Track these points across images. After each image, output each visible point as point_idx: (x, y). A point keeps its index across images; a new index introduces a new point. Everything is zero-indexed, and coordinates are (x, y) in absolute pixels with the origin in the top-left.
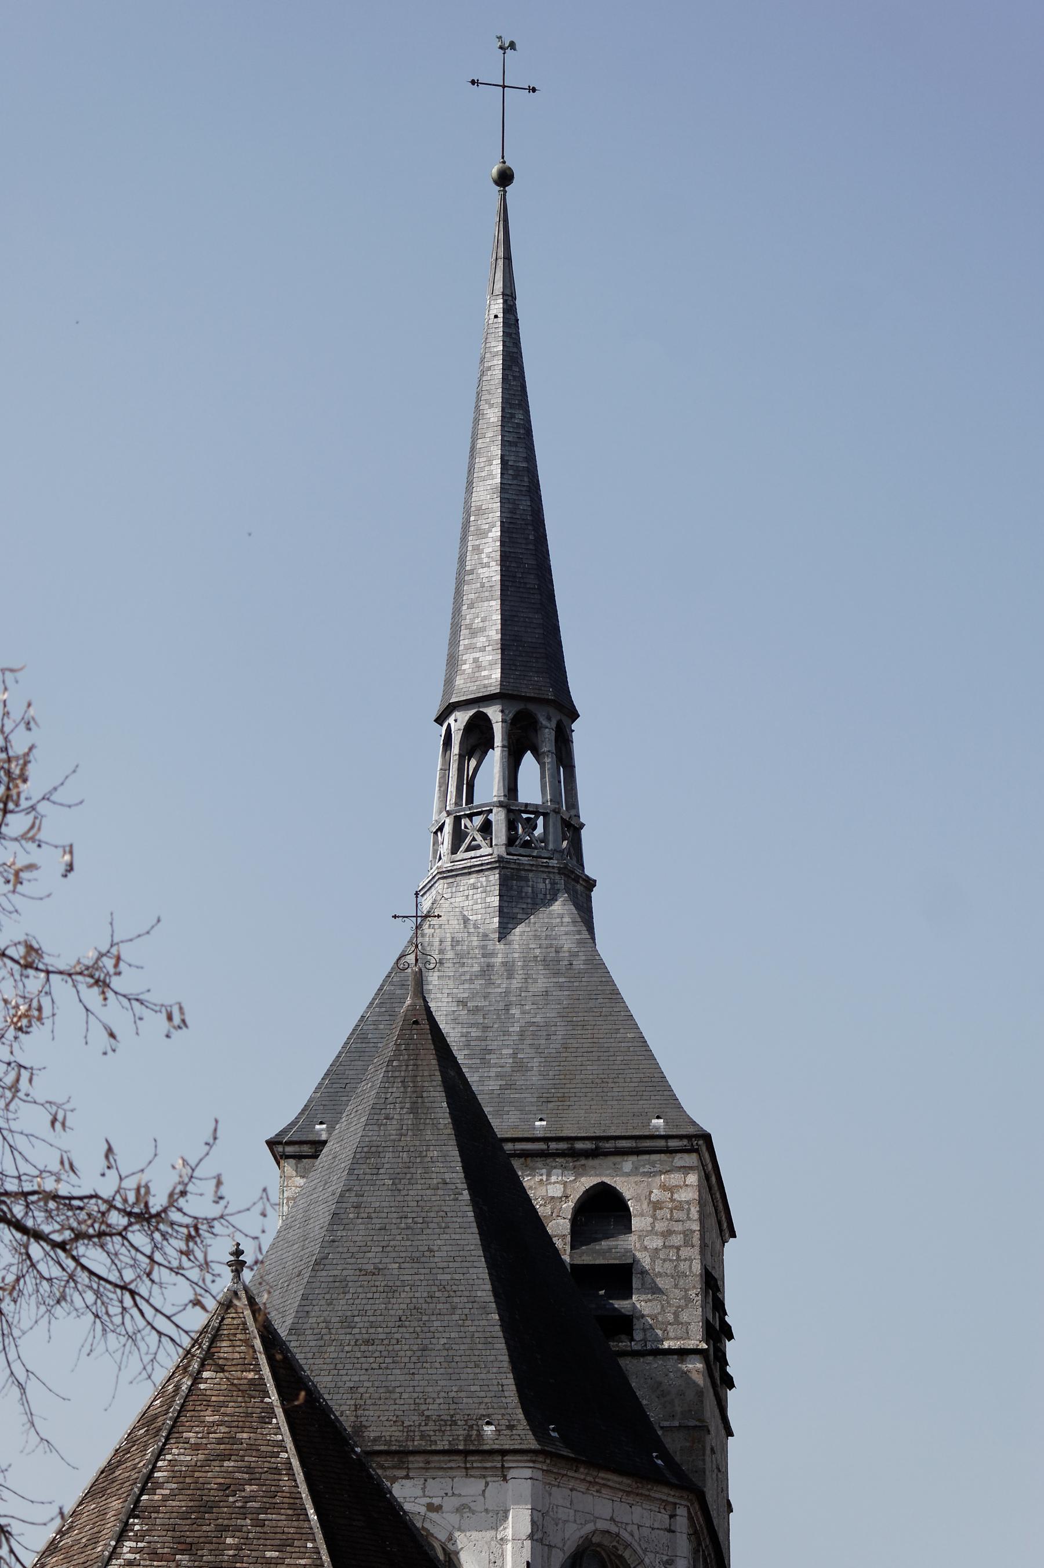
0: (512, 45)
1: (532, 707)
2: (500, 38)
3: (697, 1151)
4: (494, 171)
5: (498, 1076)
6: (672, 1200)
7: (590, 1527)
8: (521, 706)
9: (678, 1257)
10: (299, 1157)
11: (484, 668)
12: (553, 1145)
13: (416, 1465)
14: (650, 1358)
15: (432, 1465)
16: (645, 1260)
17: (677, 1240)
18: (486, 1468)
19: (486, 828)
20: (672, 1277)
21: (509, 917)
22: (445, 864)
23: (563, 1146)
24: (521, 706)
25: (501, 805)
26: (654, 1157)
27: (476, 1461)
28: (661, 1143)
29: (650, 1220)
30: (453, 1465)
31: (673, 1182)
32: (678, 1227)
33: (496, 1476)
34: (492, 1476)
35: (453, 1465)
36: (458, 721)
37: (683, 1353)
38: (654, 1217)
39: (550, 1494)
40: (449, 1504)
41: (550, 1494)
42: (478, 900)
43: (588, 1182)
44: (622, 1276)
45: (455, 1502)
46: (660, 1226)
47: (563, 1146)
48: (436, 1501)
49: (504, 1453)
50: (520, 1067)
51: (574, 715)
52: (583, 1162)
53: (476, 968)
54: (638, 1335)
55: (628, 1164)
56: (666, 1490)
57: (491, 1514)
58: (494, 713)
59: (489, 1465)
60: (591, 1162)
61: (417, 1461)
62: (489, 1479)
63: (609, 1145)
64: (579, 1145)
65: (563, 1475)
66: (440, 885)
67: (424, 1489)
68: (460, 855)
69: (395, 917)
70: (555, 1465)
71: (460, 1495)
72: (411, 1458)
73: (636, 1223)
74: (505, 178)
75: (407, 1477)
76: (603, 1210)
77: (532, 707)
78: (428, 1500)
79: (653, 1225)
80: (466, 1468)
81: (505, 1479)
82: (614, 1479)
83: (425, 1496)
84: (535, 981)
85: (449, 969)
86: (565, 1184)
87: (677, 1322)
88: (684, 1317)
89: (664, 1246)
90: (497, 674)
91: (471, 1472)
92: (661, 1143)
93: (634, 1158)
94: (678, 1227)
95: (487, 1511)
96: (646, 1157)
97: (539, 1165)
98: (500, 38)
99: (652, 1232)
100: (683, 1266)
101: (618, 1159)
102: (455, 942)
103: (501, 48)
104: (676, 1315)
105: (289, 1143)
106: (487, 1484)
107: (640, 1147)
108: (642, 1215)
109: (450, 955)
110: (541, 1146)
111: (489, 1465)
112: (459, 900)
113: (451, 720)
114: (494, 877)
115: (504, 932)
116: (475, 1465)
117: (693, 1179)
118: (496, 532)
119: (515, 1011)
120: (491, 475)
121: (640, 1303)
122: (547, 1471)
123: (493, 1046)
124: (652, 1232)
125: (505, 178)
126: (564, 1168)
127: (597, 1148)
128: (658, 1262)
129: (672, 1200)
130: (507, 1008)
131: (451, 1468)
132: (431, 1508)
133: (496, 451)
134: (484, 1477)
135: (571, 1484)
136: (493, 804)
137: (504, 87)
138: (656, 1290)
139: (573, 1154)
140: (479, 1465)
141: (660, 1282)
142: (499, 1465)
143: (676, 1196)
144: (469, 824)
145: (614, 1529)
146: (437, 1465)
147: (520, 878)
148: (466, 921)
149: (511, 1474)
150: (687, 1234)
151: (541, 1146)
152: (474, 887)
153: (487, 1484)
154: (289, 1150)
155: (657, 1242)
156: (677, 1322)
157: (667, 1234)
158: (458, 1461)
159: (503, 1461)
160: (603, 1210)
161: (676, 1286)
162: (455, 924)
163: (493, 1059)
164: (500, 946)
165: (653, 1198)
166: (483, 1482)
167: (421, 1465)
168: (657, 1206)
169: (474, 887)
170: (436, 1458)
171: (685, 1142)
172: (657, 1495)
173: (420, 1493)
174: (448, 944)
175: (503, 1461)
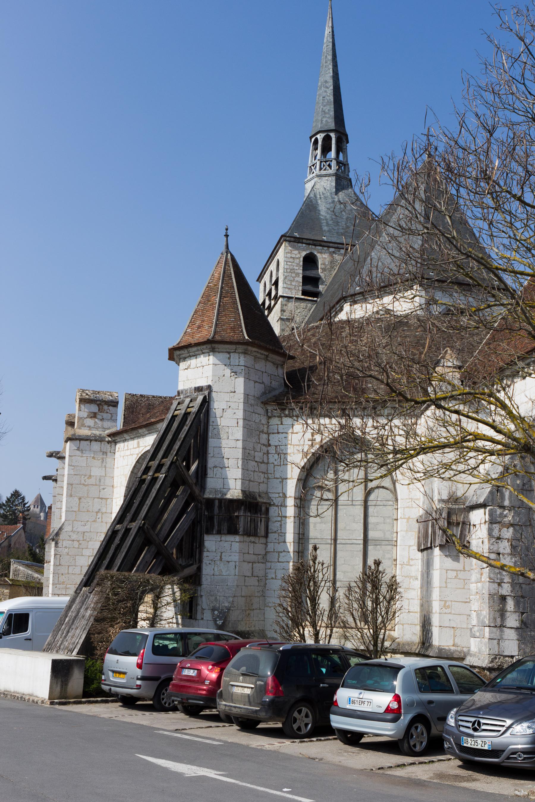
5: (342, 229)
10: (290, 241)
19: (330, 166)
25: (335, 159)
36: (320, 137)
53: (330, 201)
58: (333, 135)
66: (316, 179)
68: (322, 171)
90: (333, 124)
102: (323, 194)
105: (288, 237)
112: (322, 183)
113: (318, 136)
114: (334, 178)
118: (332, 87)
120: (329, 72)
123: (339, 221)
136: (333, 159)
144: (325, 163)
148: (325, 189)
152: (327, 180)
154: (288, 239)
162: (322, 190)
164: (336, 197)
169: (327, 180)
174: (321, 194)
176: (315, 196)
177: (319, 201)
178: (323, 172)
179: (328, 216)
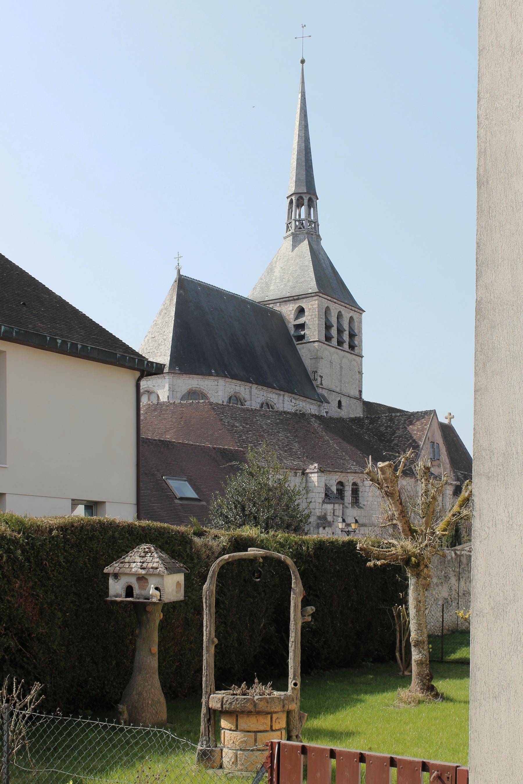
1: (302, 195)
7: (190, 387)
8: (299, 195)
12: (290, 298)
16: (307, 322)
17: (313, 316)
21: (294, 246)
24: (299, 195)
32: (314, 314)
37: (314, 342)
43: (297, 305)
44: (302, 326)
45: (157, 384)
46: (310, 314)
47: (292, 298)
50: (289, 281)
54: (306, 339)
55: (304, 300)
60: (298, 301)
63: (300, 297)
64: (295, 298)
73: (306, 314)
76: (301, 311)
77: (302, 195)
88: (314, 334)
92: (310, 295)
94: (314, 314)
100: (314, 322)
114: (291, 237)
115: (293, 250)
117: (317, 302)
121: (306, 331)
138: (309, 328)
139: (294, 300)
141: (311, 327)
145: (198, 386)
147: (297, 237)
150: (315, 315)
155: (310, 318)
157: (312, 315)
160: (301, 311)
168: (310, 309)
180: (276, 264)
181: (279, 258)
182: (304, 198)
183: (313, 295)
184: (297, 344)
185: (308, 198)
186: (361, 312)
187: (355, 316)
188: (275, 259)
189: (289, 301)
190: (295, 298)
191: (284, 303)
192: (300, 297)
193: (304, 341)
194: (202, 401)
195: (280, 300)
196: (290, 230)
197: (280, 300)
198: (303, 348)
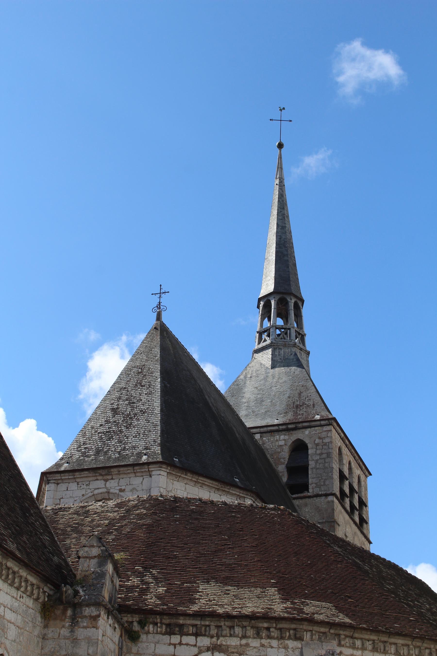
0: (284, 109)
1: (285, 296)
2: (280, 107)
3: (331, 425)
4: (277, 144)
6: (323, 442)
9: (325, 461)
11: (268, 286)
12: (281, 427)
13: (115, 473)
14: (315, 498)
15: (121, 472)
17: (324, 456)
18: (142, 472)
20: (323, 469)
22: (256, 348)
23: (284, 427)
24: (281, 296)
26: (316, 428)
27: (138, 469)
28: (318, 423)
29: (315, 450)
30: (129, 471)
31: (323, 436)
33: (147, 475)
34: (146, 475)
35: (129, 471)
38: (316, 449)
39: (173, 484)
40: (128, 488)
41: (173, 484)
42: (266, 357)
45: (130, 487)
46: (318, 452)
47: (284, 427)
48: (123, 488)
49: (148, 464)
51: (303, 301)
52: (291, 432)
54: (310, 490)
56: (238, 490)
57: (144, 491)
59: (143, 470)
60: (294, 432)
61: (114, 471)
62: (144, 477)
63: (300, 425)
64: (290, 426)
65: (180, 476)
67: (118, 483)
69: (152, 294)
70: (173, 471)
71: (132, 484)
72: (112, 470)
74: (280, 146)
75: (112, 479)
77: (285, 296)
78: (120, 487)
79: (316, 452)
80: (135, 473)
81: (151, 476)
82: (208, 482)
83: (119, 486)
84: (282, 379)
85: (253, 379)
86: (284, 440)
87: (324, 485)
89: (320, 459)
91: (138, 474)
92: (318, 423)
93: (309, 429)
95: (143, 490)
96: (313, 428)
97: (276, 435)
98: (280, 107)
99: (316, 454)
101: (304, 430)
103: (280, 110)
104: (324, 482)
106: (143, 479)
107: (310, 424)
108: (312, 448)
109: (254, 374)
110: (276, 428)
111: (143, 470)
116: (138, 471)
119: (274, 388)
122: (168, 473)
124: (316, 454)
125: (280, 146)
126: (285, 435)
127: (296, 427)
128: (318, 464)
129: (323, 442)
130: (271, 388)
131: (129, 473)
132: (121, 490)
133: (275, 222)
134: (142, 476)
135: (186, 481)
137: (281, 120)
139: (288, 430)
140: (139, 471)
142: (147, 470)
143: (324, 441)
146: (123, 472)
149: (153, 473)
151: (276, 428)
153: (143, 479)
155: (318, 457)
156: (324, 485)
157: (321, 454)
158: (130, 469)
159: (148, 468)
161: (324, 472)
163: (264, 403)
165: (316, 442)
166: (142, 478)
167: (117, 473)
168: (317, 445)
170: (122, 469)
171: (327, 421)
172: (234, 492)
173: (117, 485)
175: (148, 468)
176: (245, 377)
177: (248, 382)
178: (263, 344)
179: (253, 397)
180: (245, 383)
181: (249, 376)
182: (289, 300)
183: (323, 422)
184: (295, 498)
185: (293, 301)
186: (367, 473)
187: (362, 477)
188: (242, 377)
189: (278, 431)
190: (290, 426)
191: (268, 434)
192: (300, 425)
193: (306, 494)
194: (272, 506)
195: (262, 430)
196: (265, 340)
197: (262, 430)
198: (306, 505)
